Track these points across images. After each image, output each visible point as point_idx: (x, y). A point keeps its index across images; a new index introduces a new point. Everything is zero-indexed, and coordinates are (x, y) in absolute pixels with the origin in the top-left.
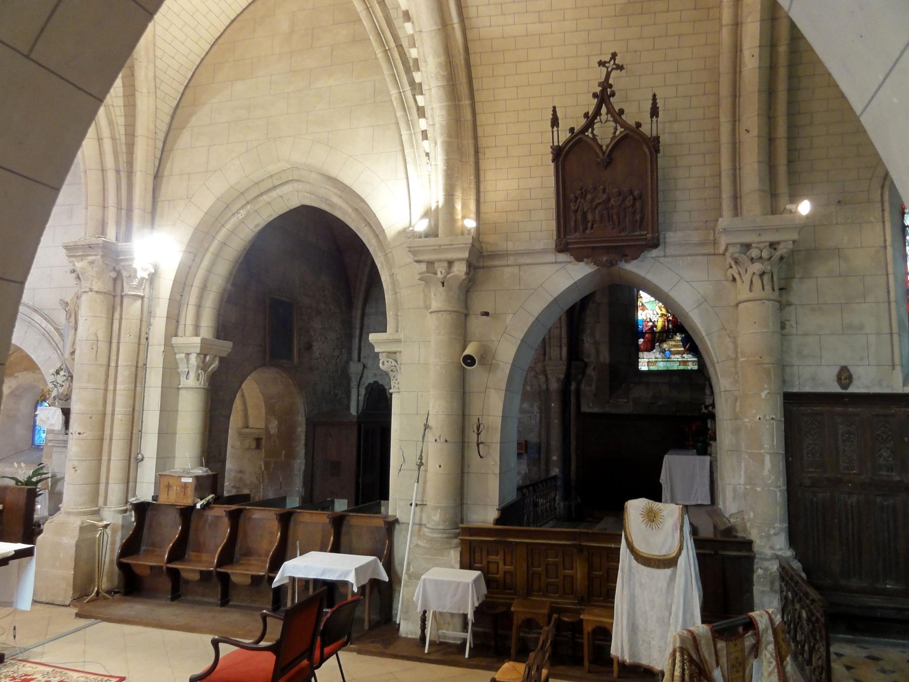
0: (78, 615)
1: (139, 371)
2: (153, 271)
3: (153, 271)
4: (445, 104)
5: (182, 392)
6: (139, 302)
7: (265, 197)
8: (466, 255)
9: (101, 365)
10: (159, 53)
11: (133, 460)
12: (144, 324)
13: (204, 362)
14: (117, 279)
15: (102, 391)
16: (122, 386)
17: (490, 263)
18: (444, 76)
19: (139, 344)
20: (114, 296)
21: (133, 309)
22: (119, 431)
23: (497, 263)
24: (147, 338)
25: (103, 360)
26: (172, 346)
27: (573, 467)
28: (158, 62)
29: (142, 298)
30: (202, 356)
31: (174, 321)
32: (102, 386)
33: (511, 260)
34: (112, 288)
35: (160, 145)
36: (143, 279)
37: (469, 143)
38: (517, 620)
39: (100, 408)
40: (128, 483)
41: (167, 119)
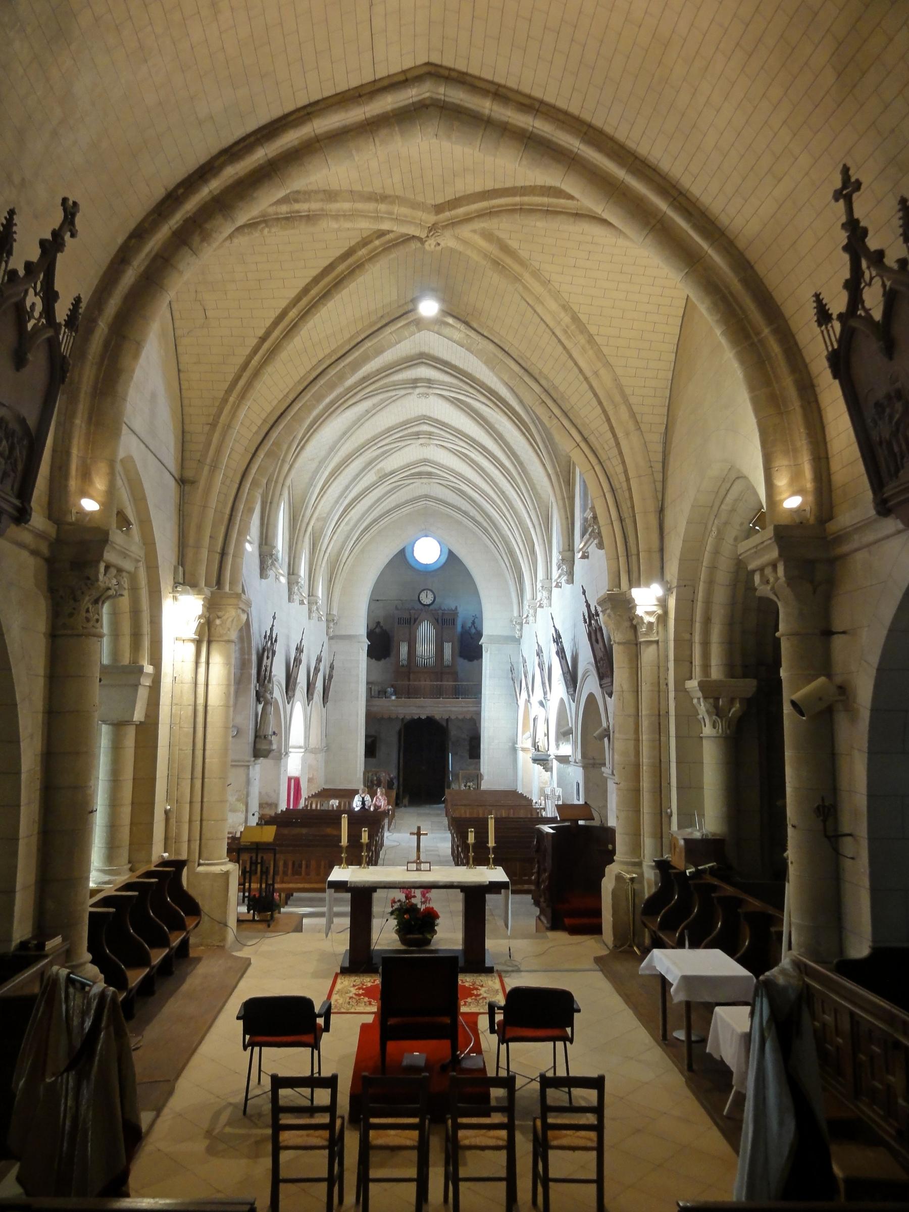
0: (598, 960)
1: (660, 719)
2: (660, 612)
3: (660, 612)
4: (734, 351)
5: (704, 742)
6: (652, 649)
7: (723, 507)
8: (775, 554)
9: (629, 716)
10: (628, 391)
11: (661, 816)
12: (662, 669)
13: (716, 707)
14: (634, 628)
15: (632, 742)
16: (645, 737)
17: (845, 548)
18: (717, 321)
19: (659, 692)
20: (636, 645)
21: (648, 655)
22: (646, 784)
23: (845, 548)
24: (667, 685)
25: (631, 710)
26: (686, 691)
27: (307, 886)
28: (632, 400)
29: (657, 642)
30: (711, 701)
31: (688, 664)
32: (631, 735)
33: (857, 541)
34: (633, 638)
35: (659, 477)
36: (650, 624)
37: (788, 383)
38: (62, 980)
39: (632, 758)
40: (662, 838)
41: (660, 448)
